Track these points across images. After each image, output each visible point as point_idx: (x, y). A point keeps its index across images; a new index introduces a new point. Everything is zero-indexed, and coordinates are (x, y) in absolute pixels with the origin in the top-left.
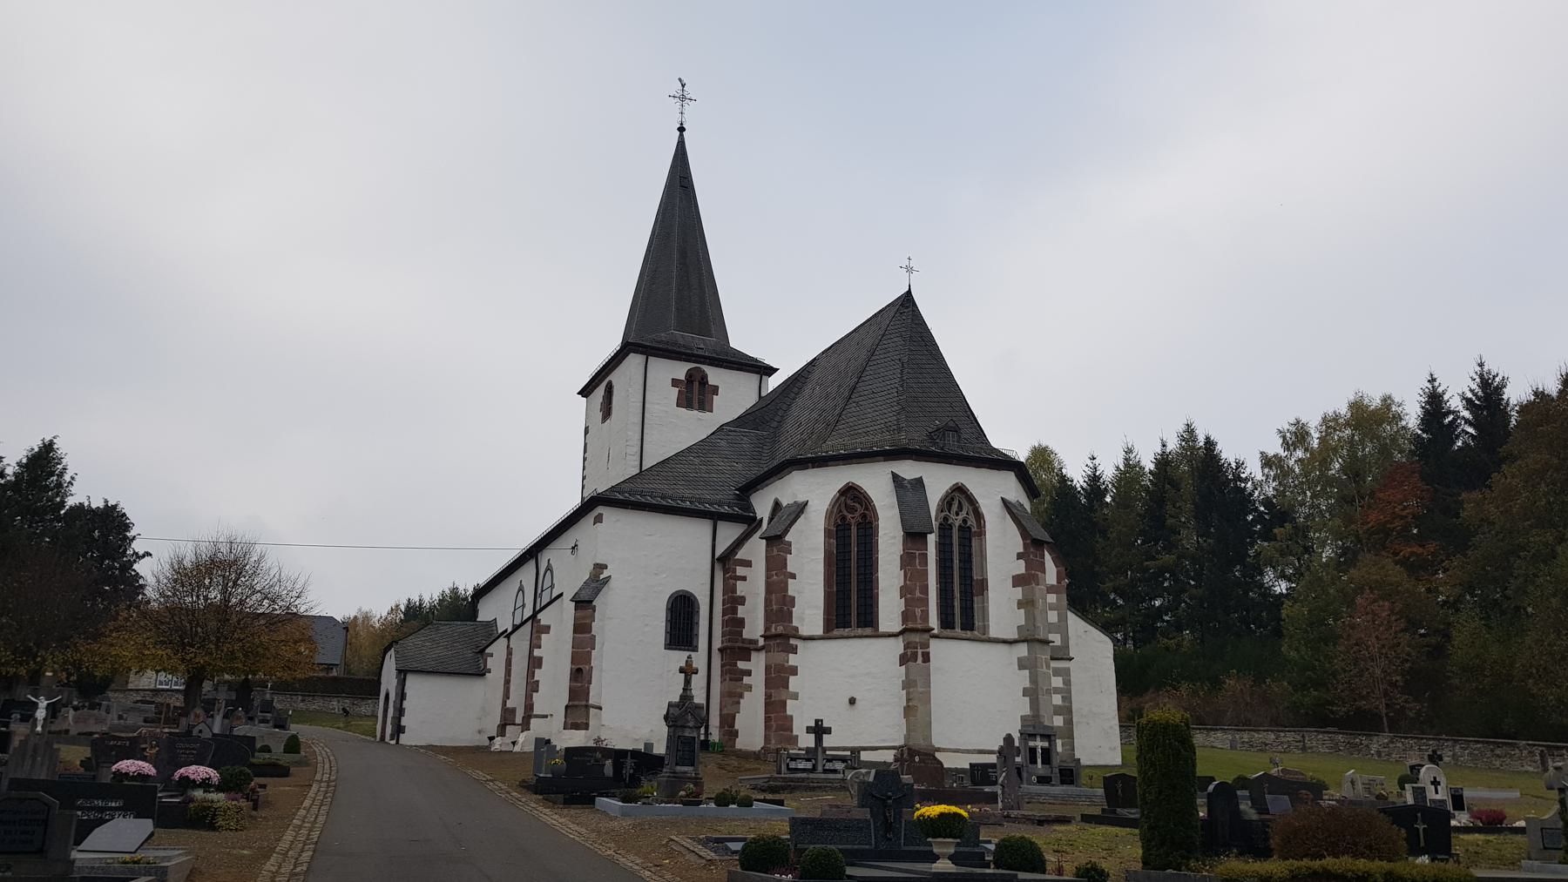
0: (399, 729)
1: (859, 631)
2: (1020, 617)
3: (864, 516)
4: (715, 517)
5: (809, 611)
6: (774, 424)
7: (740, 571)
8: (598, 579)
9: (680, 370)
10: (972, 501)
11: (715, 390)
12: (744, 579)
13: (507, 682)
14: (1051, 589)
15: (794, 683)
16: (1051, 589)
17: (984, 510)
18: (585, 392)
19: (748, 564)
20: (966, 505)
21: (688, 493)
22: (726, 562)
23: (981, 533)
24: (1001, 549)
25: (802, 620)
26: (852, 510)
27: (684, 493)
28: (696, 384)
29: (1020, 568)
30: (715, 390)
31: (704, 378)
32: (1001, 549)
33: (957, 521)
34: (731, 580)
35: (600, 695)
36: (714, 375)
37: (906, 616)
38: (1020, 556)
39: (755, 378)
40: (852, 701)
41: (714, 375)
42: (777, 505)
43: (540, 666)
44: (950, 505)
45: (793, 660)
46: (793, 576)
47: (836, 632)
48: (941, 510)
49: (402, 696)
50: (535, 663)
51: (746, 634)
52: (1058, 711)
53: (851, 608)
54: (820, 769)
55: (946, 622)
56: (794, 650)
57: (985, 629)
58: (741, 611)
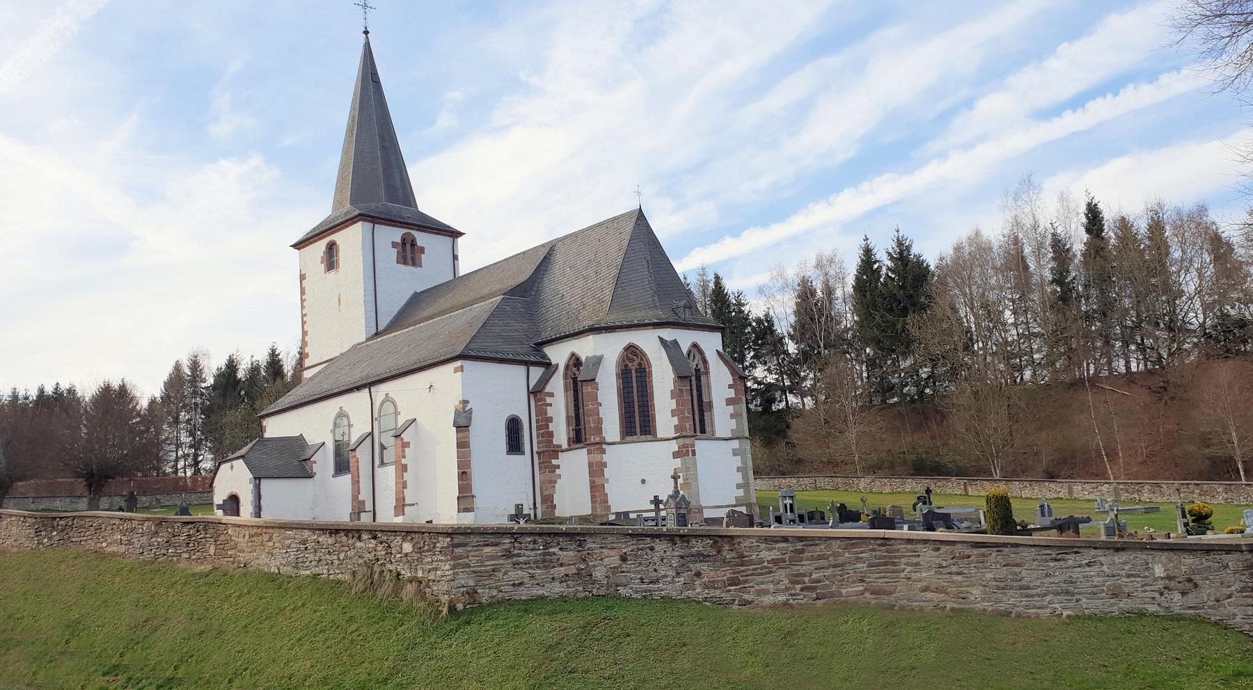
1: (643, 437)
3: (640, 364)
4: (528, 364)
7: (549, 400)
10: (701, 352)
11: (422, 250)
12: (550, 405)
17: (708, 358)
18: (299, 245)
19: (551, 395)
22: (537, 393)
23: (707, 373)
26: (632, 360)
28: (408, 246)
30: (422, 250)
31: (413, 244)
36: (421, 238)
38: (730, 387)
39: (449, 240)
40: (643, 481)
41: (421, 238)
47: (628, 438)
51: (555, 442)
57: (713, 432)
58: (551, 427)
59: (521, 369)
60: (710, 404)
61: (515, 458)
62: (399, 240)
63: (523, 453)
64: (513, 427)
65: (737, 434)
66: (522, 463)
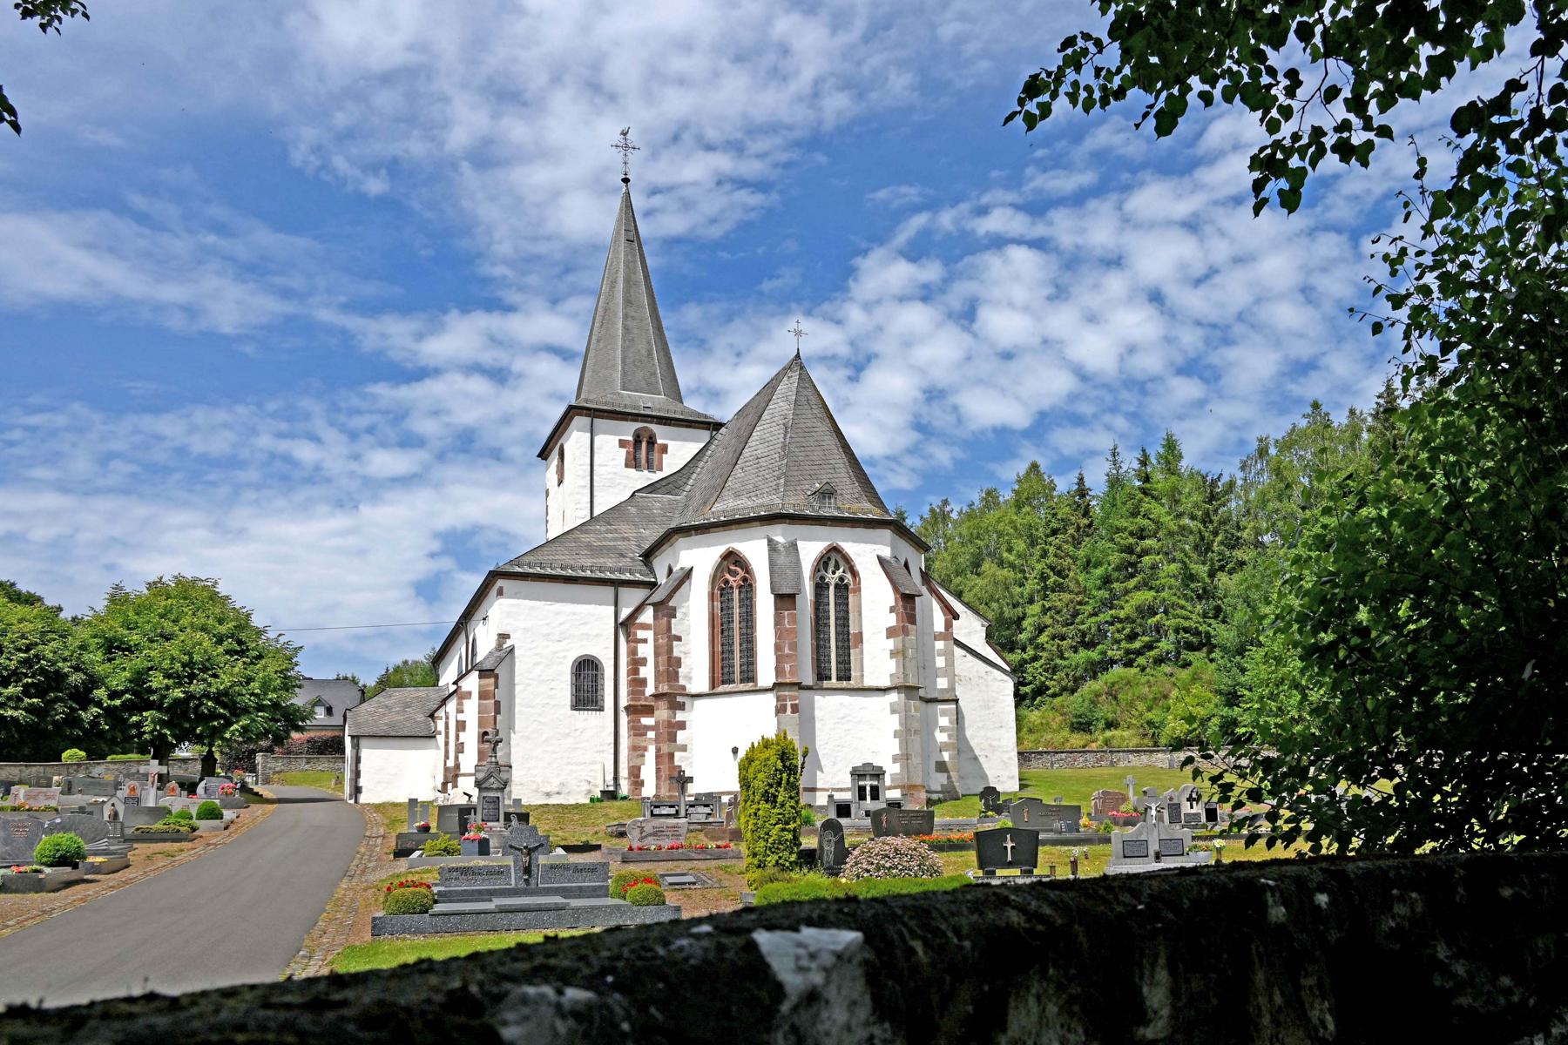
0: (357, 790)
1: (742, 687)
2: (891, 666)
3: (745, 580)
5: (696, 670)
6: (688, 488)
7: (641, 634)
8: (505, 653)
9: (628, 430)
10: (847, 560)
12: (645, 641)
13: (447, 744)
15: (681, 736)
17: (859, 567)
20: (841, 562)
21: (588, 562)
22: (626, 626)
24: (876, 602)
25: (689, 679)
26: (734, 574)
27: (585, 564)
28: (644, 444)
29: (892, 620)
30: (664, 449)
32: (876, 602)
33: (832, 578)
34: (633, 641)
35: (509, 754)
36: (662, 434)
37: (779, 671)
38: (892, 610)
41: (662, 434)
42: (670, 571)
43: (464, 729)
44: (826, 565)
45: (680, 716)
46: (679, 639)
47: (721, 689)
48: (816, 570)
49: (358, 760)
50: (461, 726)
53: (732, 669)
54: (683, 813)
55: (822, 675)
56: (682, 707)
59: (610, 590)
61: (587, 718)
62: (630, 438)
63: (601, 709)
64: (586, 669)
65: (900, 682)
66: (598, 723)
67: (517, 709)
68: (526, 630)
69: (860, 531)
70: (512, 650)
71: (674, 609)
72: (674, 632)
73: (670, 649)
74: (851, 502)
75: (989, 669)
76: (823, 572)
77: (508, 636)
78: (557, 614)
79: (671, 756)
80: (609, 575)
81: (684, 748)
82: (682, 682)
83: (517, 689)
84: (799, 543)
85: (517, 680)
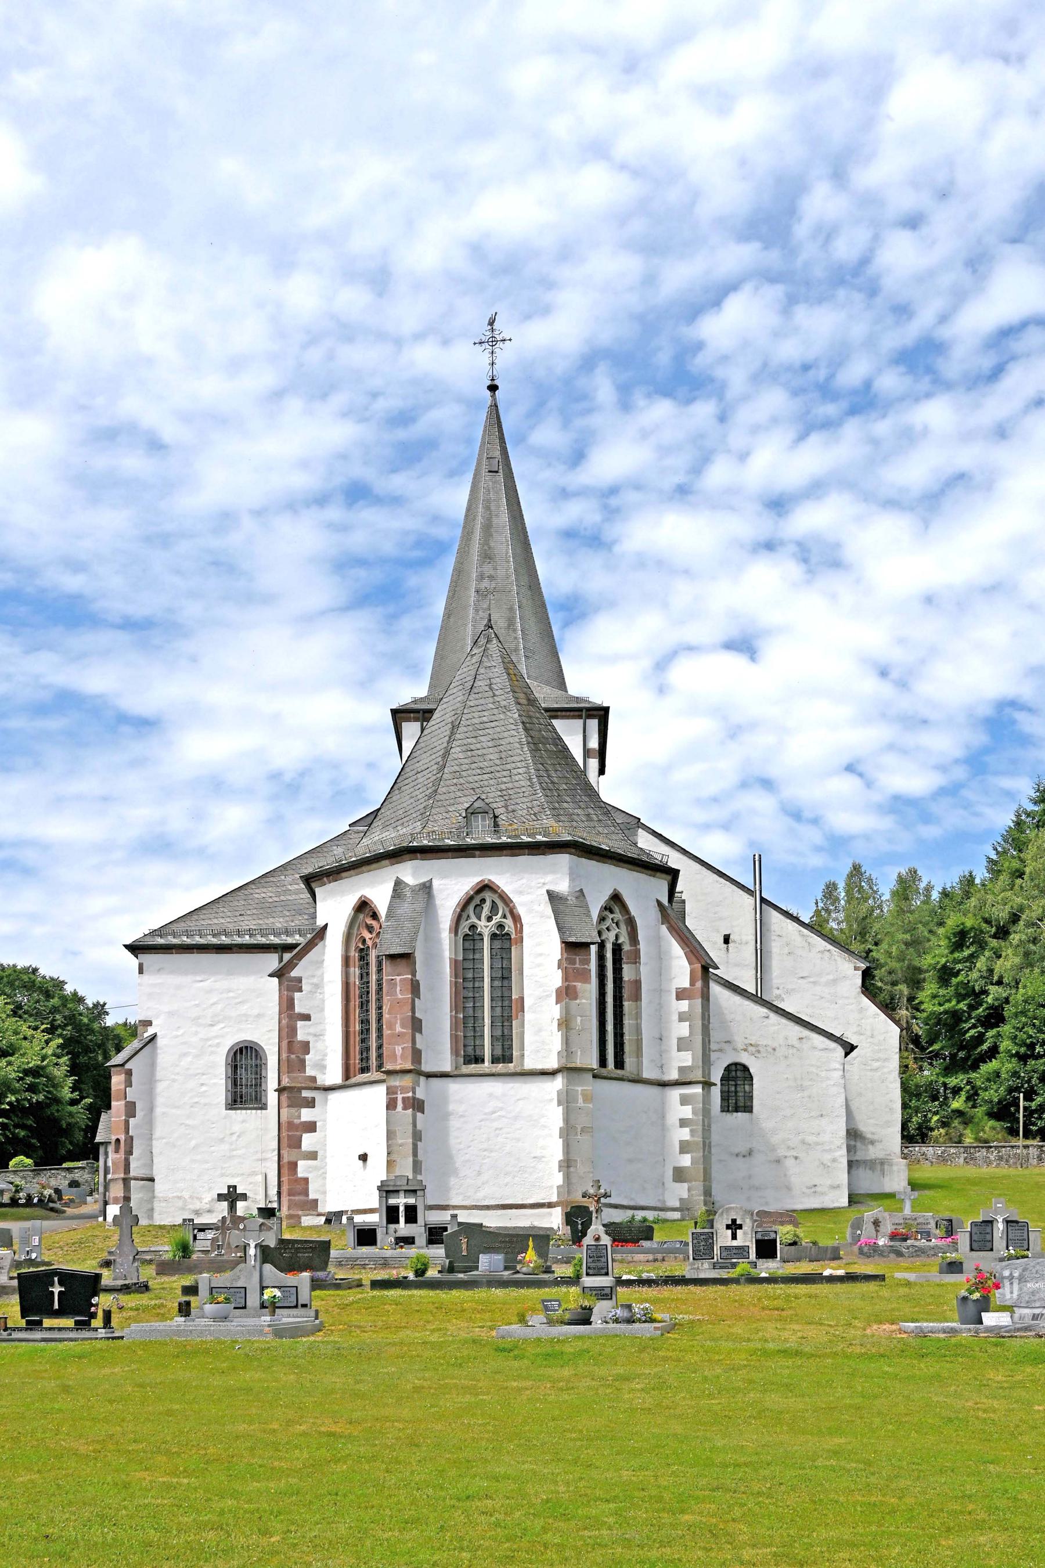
2: (555, 1041)
14: (681, 994)
16: (681, 994)
17: (521, 910)
33: (485, 927)
44: (479, 907)
45: (306, 1115)
46: (307, 1017)
52: (685, 1147)
56: (311, 1103)
60: (522, 999)
63: (264, 1107)
64: (244, 1059)
67: (159, 1111)
68: (171, 1014)
69: (524, 860)
70: (153, 1038)
71: (299, 980)
72: (298, 1009)
73: (293, 1031)
74: (531, 816)
75: (806, 1033)
76: (474, 919)
77: (149, 1023)
78: (210, 991)
79: (293, 1166)
80: (274, 940)
81: (313, 1156)
82: (310, 1072)
83: (160, 1087)
84: (436, 884)
85: (159, 1074)
